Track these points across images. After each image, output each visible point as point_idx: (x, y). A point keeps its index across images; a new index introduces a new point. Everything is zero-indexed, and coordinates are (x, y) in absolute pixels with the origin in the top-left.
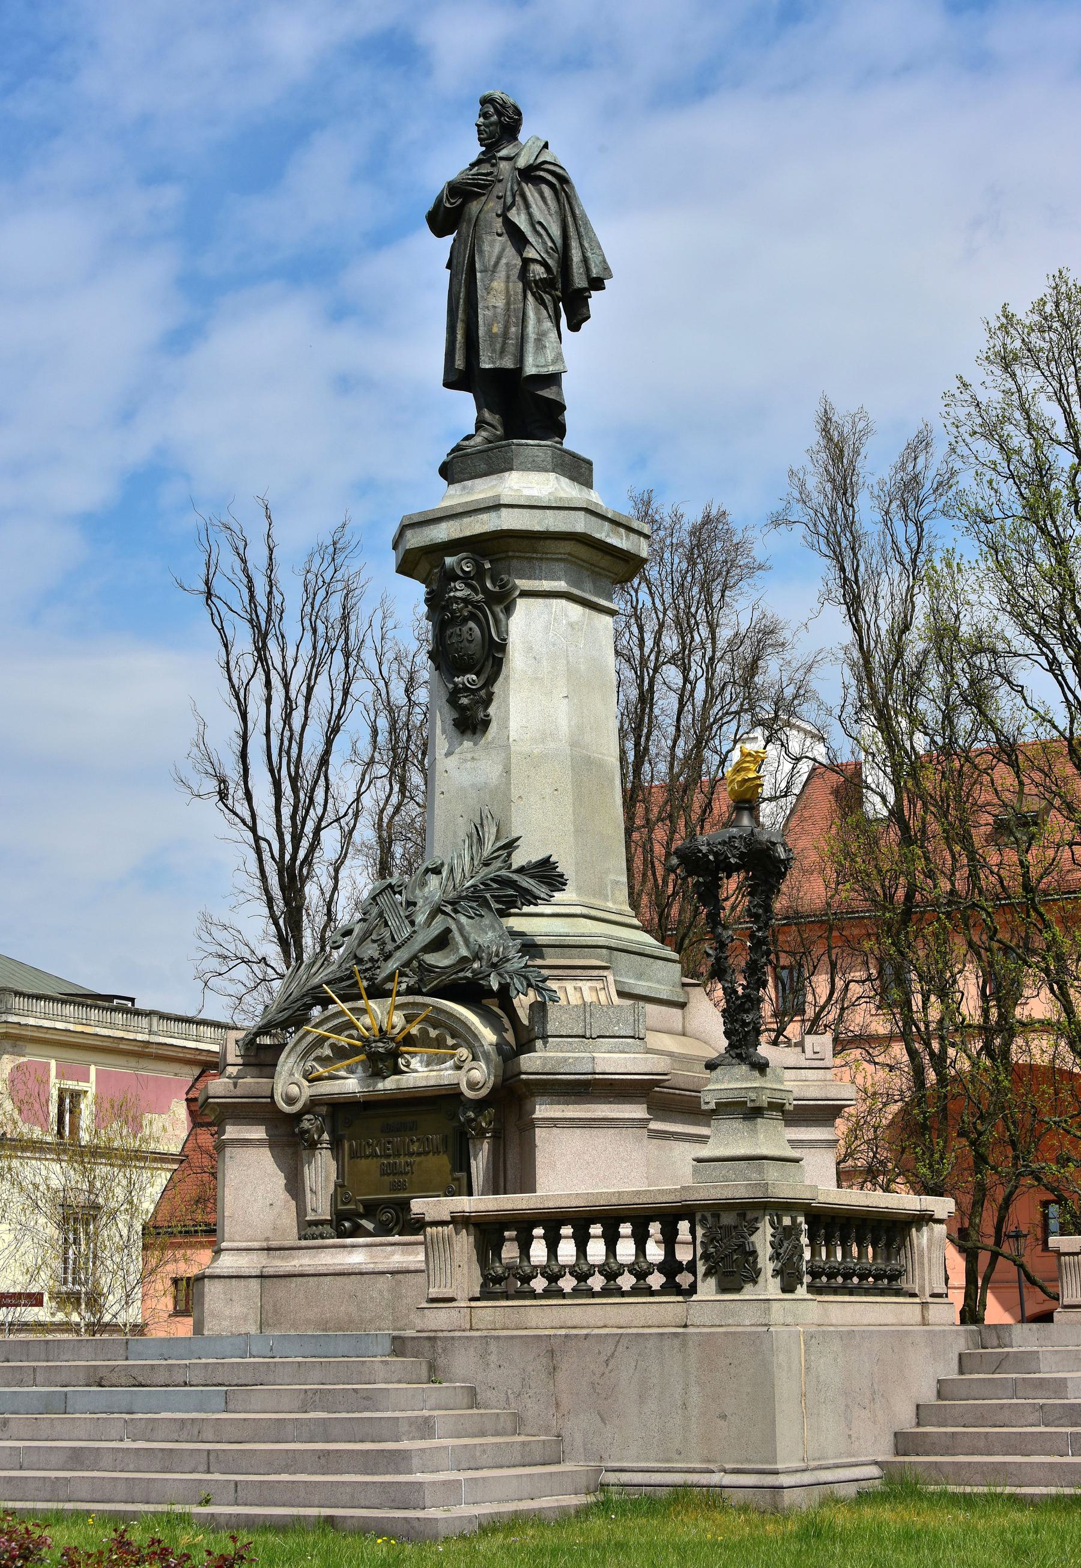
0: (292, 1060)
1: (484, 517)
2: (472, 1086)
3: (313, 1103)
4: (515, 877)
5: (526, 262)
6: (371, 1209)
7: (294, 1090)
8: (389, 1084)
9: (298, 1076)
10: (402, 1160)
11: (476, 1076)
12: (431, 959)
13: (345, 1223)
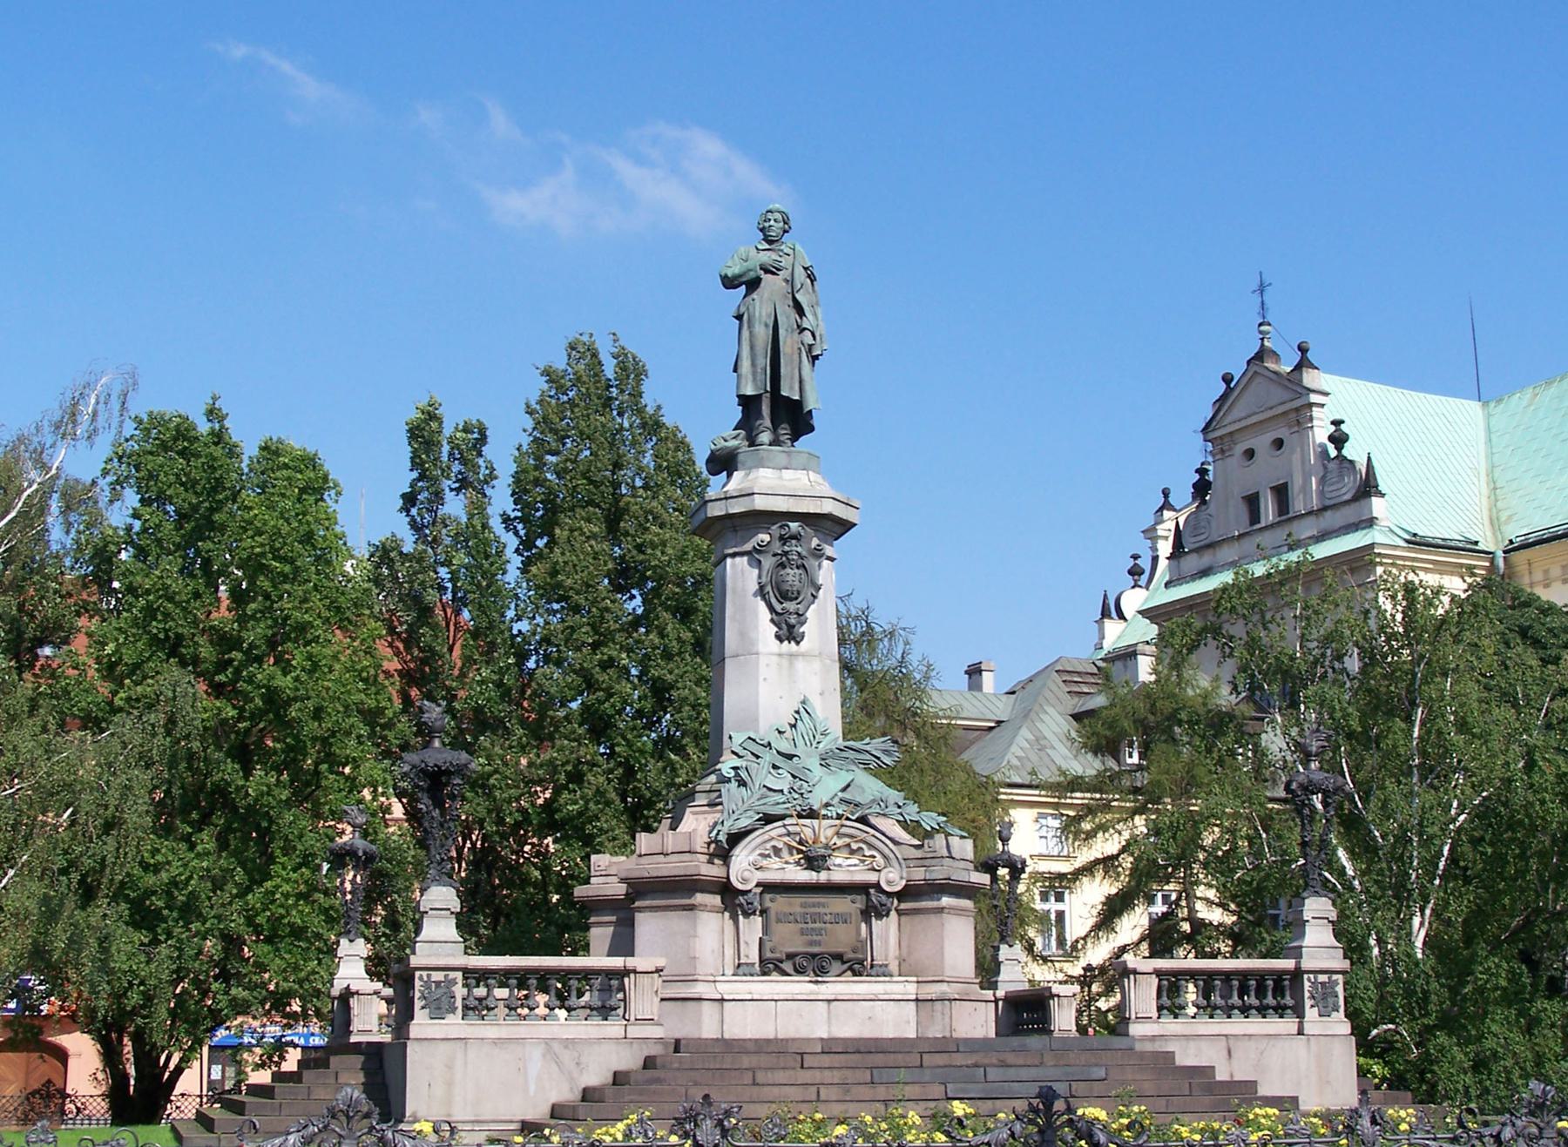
0: (745, 852)
1: (818, 501)
2: (889, 883)
3: (758, 885)
4: (867, 748)
5: (802, 330)
6: (790, 956)
7: (746, 874)
8: (823, 877)
9: (745, 865)
10: (817, 925)
11: (893, 879)
12: (846, 795)
13: (769, 965)
